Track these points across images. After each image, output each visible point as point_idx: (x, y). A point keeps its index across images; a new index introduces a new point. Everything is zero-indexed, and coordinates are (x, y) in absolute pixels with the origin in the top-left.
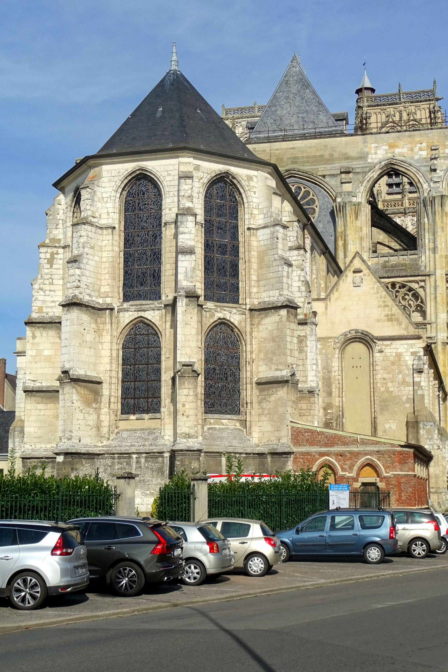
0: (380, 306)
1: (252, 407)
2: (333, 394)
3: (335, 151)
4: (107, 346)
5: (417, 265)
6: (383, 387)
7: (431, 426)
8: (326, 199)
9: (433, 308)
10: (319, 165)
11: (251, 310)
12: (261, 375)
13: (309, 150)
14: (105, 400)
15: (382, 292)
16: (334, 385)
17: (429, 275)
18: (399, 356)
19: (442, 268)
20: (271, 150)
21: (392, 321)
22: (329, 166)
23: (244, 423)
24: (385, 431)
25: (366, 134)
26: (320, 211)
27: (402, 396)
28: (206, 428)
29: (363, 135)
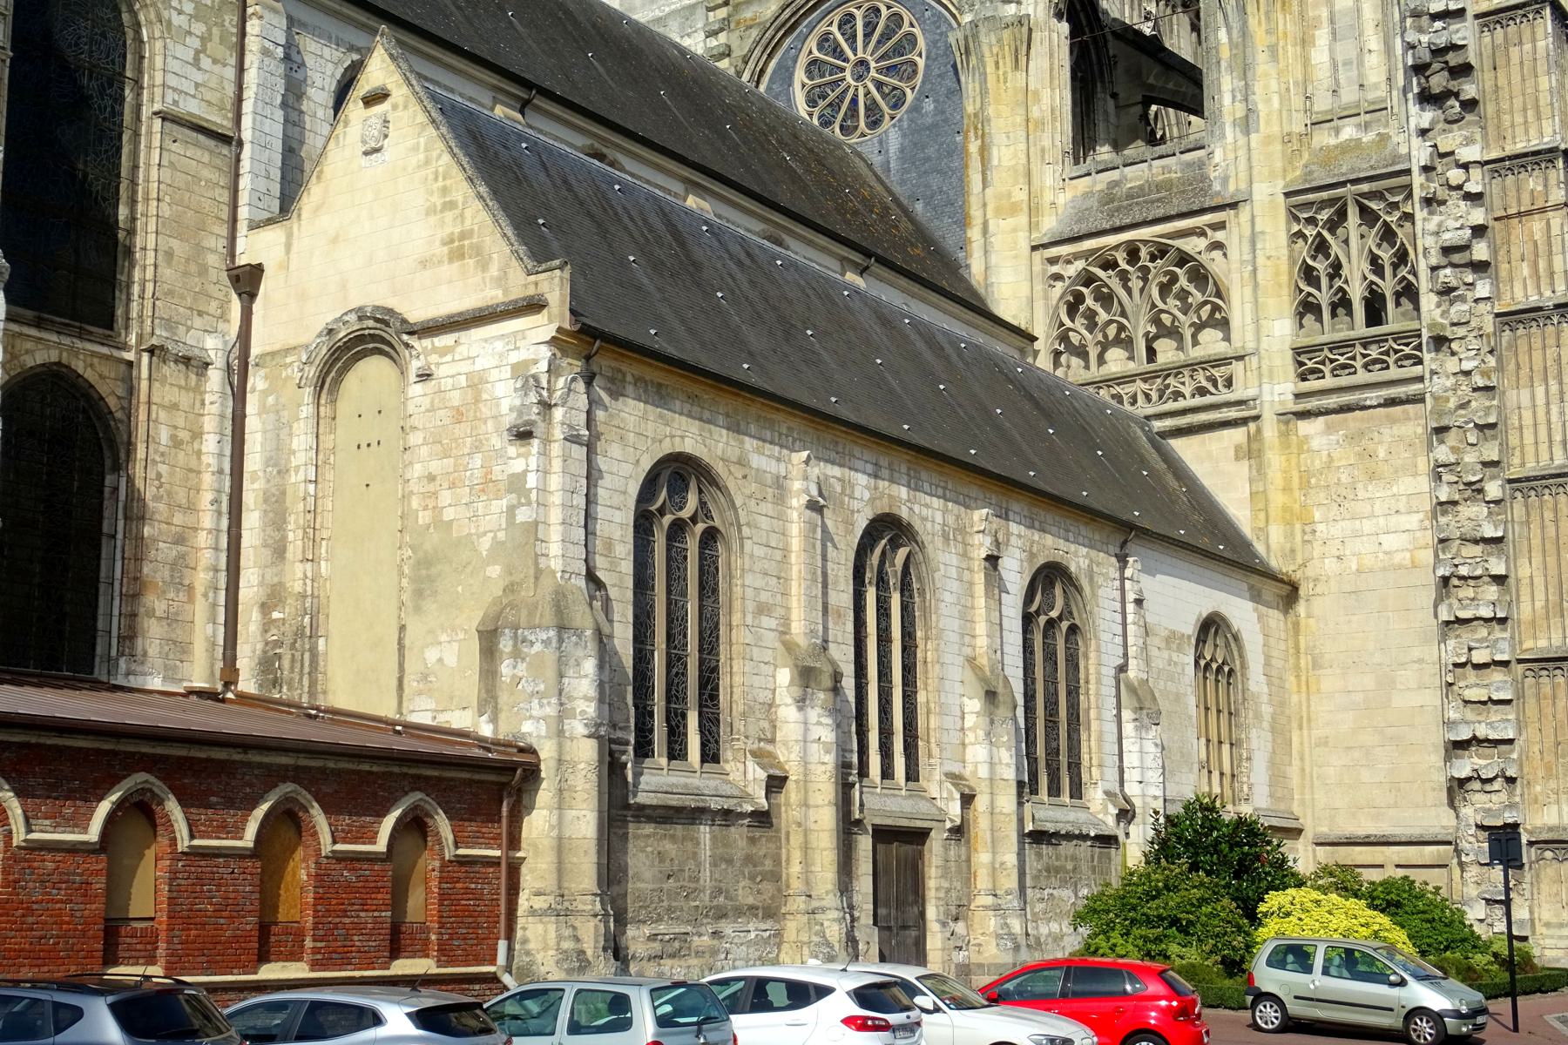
0: (431, 211)
2: (289, 555)
5: (1204, 178)
6: (425, 508)
7: (546, 643)
9: (1248, 307)
15: (439, 157)
16: (292, 519)
17: (1233, 205)
18: (476, 383)
19: (1272, 176)
21: (462, 256)
24: (424, 677)
26: (927, 66)
27: (479, 536)
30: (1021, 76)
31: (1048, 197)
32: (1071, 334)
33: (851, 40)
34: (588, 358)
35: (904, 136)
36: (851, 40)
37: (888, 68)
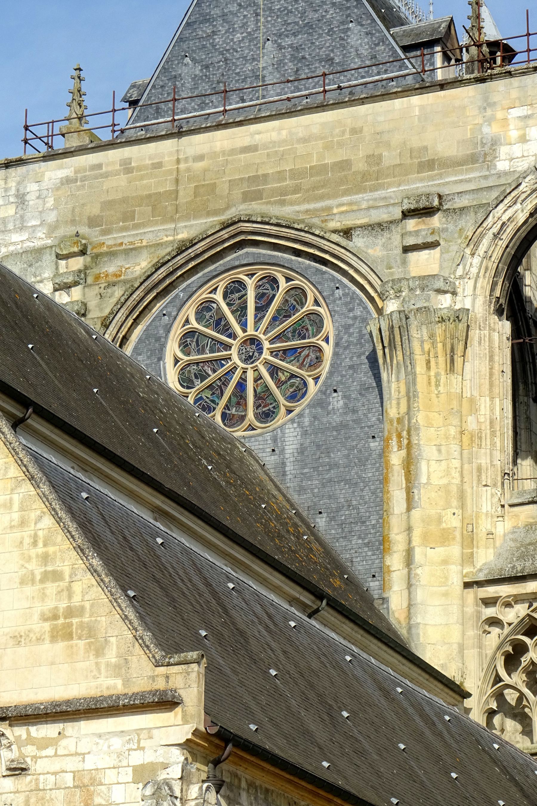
0: (27, 580)
3: (388, 145)
8: (358, 312)
10: (335, 196)
13: (301, 149)
15: (39, 519)
20: (178, 161)
21: (69, 636)
22: (367, 196)
25: (491, 77)
26: (336, 354)
29: (481, 80)
30: (455, 379)
31: (484, 525)
32: (506, 692)
33: (241, 312)
34: (216, 763)
35: (305, 433)
36: (241, 312)
37: (285, 351)
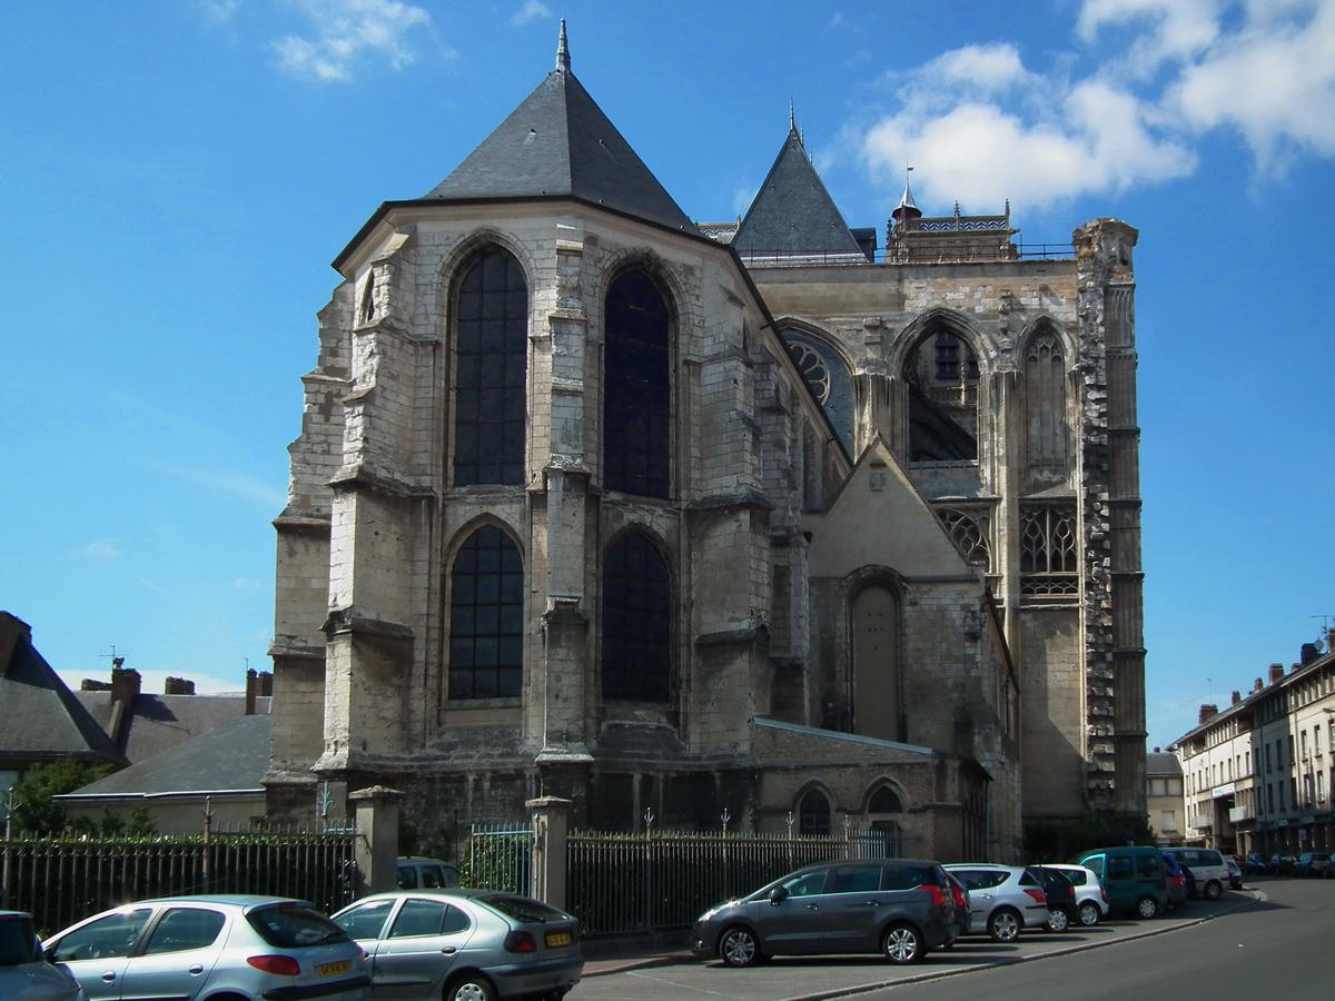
1: (689, 686)
4: (423, 568)
11: (688, 511)
12: (707, 630)
14: (418, 670)
23: (674, 718)
28: (604, 727)
